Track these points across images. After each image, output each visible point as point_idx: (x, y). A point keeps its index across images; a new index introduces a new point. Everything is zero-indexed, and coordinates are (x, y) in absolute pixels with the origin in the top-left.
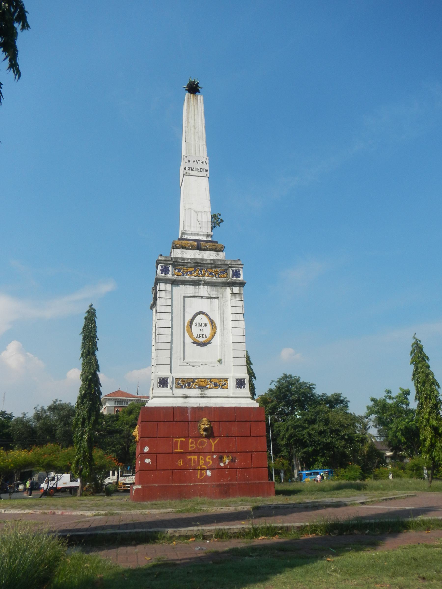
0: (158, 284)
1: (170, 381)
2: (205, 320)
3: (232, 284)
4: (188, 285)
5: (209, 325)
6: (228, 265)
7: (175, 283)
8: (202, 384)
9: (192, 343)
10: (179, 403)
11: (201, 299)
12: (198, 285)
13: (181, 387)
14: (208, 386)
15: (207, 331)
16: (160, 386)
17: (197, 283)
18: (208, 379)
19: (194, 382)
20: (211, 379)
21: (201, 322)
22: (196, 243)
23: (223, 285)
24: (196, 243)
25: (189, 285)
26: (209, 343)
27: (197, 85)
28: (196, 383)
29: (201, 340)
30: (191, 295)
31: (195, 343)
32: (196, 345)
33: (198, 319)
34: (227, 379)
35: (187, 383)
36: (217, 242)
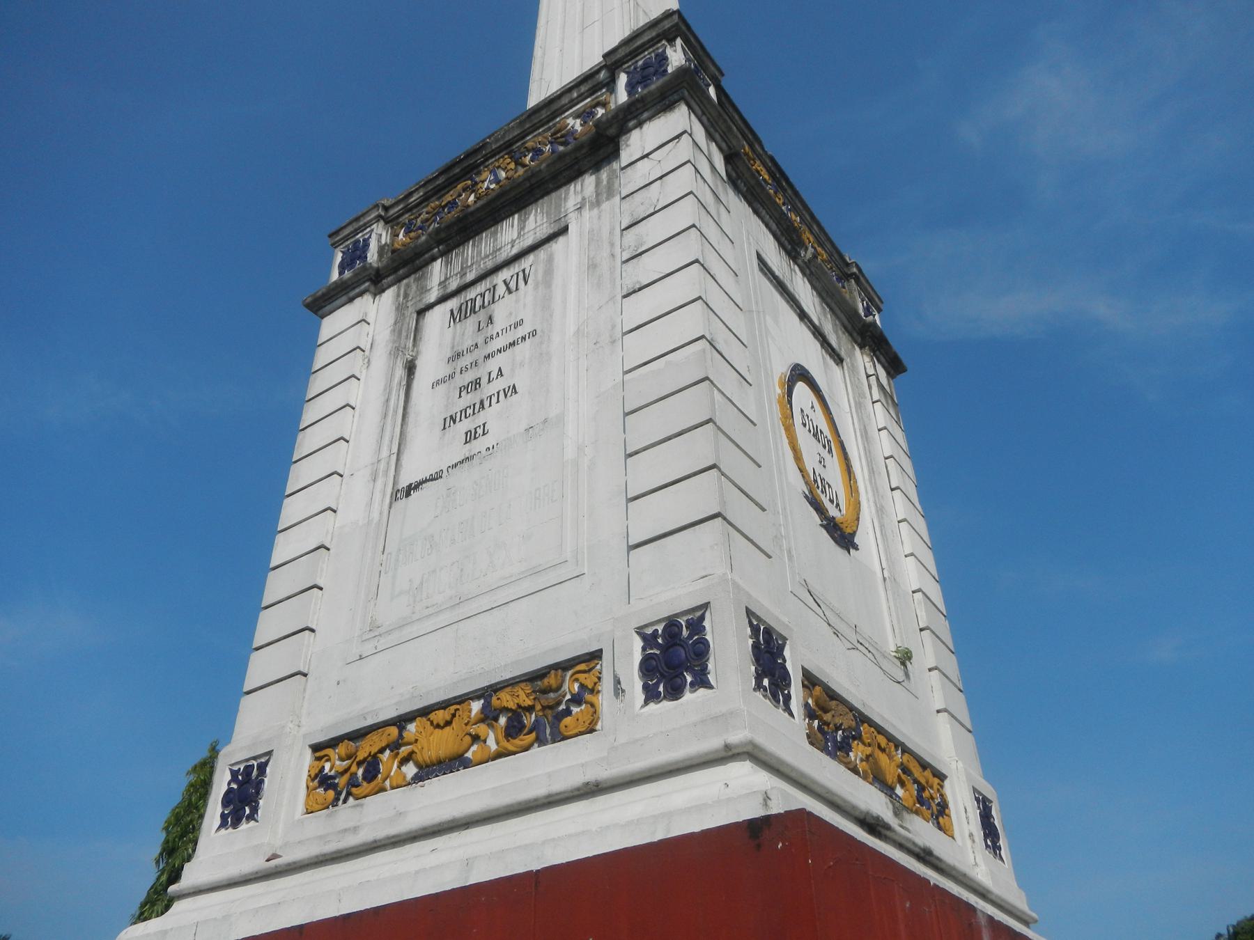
0: (683, 109)
3: (872, 340)
4: (763, 221)
6: (848, 265)
8: (883, 759)
9: (806, 497)
11: (797, 319)
12: (788, 253)
13: (824, 749)
14: (899, 791)
16: (759, 686)
17: (791, 241)
18: (898, 744)
19: (858, 737)
20: (906, 750)
23: (850, 327)
25: (767, 226)
28: (868, 750)
30: (777, 273)
32: (817, 519)
34: (941, 777)
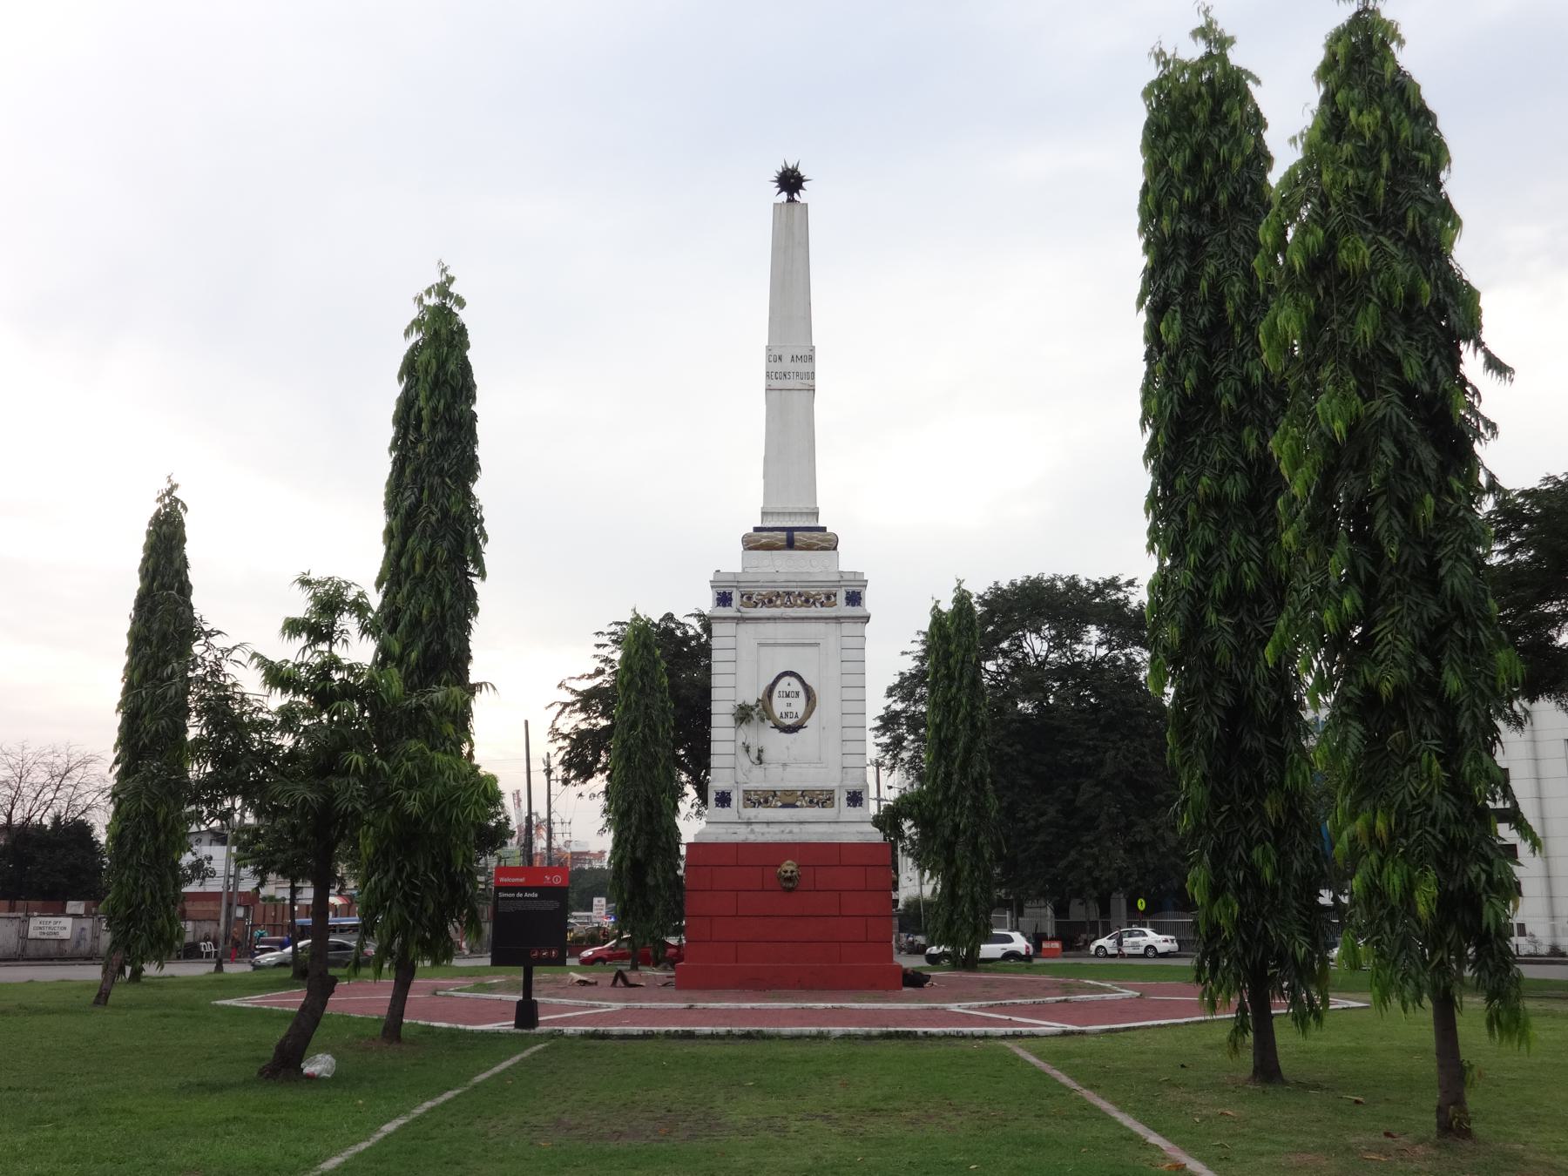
1: (734, 797)
2: (796, 685)
5: (802, 694)
7: (740, 620)
10: (742, 835)
15: (799, 705)
21: (788, 689)
22: (783, 535)
24: (783, 535)
26: (801, 727)
27: (794, 170)
29: (789, 722)
31: (776, 727)
33: (783, 685)
35: (761, 799)
36: (824, 529)
